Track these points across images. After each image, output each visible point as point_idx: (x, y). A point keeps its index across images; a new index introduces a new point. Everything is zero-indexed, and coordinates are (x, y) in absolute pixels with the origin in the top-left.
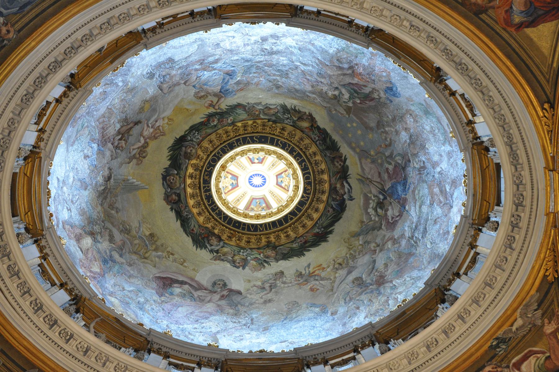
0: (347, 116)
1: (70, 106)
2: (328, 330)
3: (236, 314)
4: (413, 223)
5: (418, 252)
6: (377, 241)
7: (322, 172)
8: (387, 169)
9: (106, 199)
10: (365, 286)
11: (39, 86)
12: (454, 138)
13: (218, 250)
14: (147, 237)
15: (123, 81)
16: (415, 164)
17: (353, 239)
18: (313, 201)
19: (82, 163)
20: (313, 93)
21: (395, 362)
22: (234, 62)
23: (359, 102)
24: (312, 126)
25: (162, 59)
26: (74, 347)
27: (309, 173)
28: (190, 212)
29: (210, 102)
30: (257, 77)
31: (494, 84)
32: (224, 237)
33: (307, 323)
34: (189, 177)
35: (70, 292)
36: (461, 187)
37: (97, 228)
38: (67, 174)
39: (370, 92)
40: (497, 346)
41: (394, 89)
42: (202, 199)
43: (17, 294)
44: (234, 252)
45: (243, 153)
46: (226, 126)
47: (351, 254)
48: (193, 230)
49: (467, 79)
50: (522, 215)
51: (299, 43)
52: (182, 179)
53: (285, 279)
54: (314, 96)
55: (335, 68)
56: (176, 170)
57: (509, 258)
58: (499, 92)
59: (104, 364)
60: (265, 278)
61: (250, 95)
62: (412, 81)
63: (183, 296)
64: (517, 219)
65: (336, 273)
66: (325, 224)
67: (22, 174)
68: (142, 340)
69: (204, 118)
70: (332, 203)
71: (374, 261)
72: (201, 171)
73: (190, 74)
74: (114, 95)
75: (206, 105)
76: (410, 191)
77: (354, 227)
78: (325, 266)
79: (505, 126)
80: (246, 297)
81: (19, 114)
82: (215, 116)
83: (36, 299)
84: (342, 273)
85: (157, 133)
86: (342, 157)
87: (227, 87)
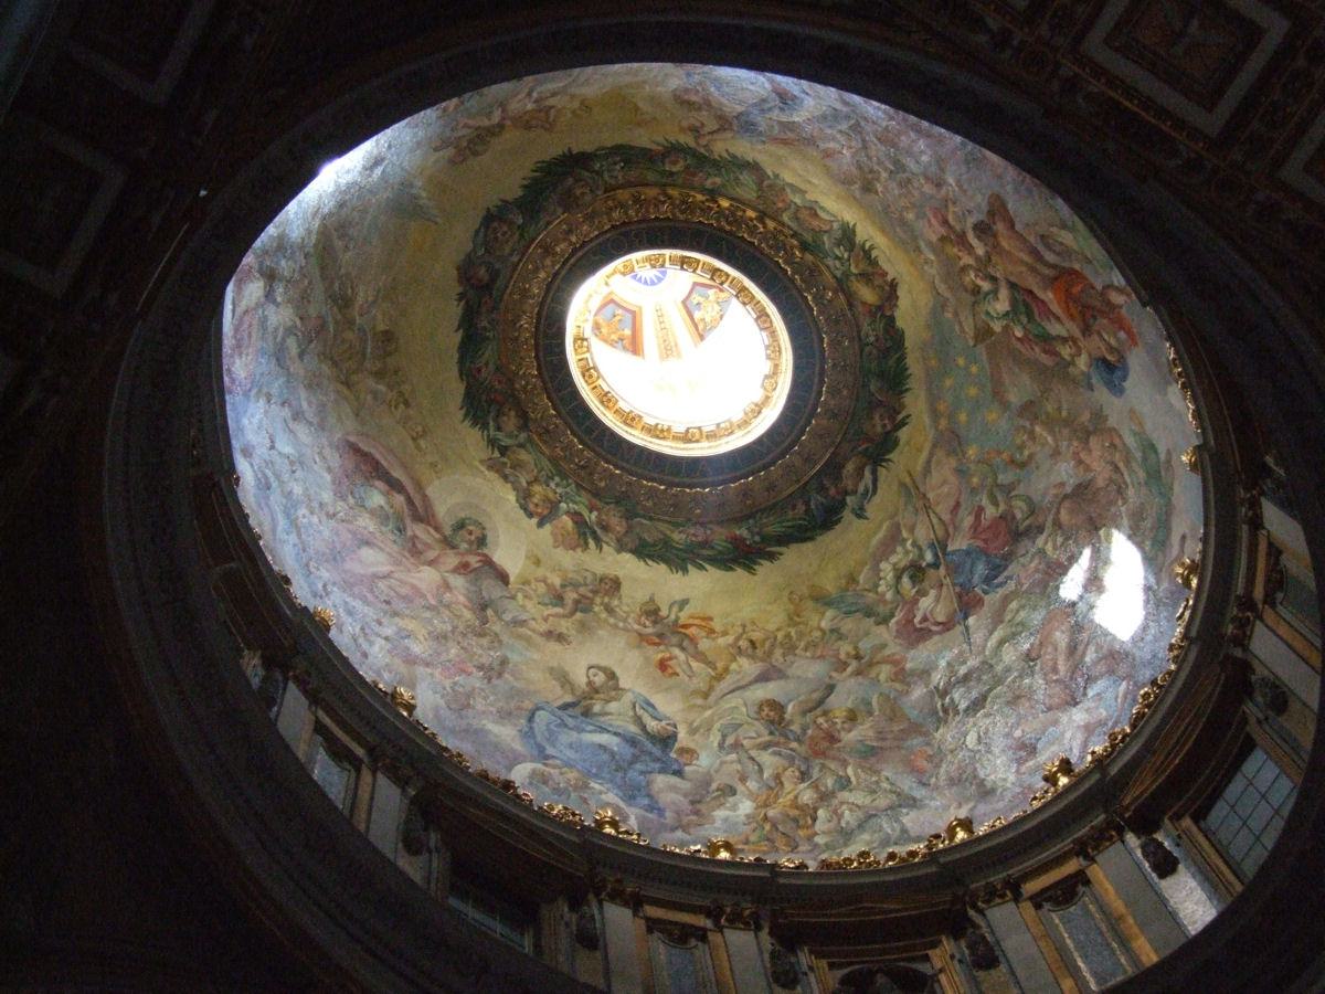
0: (971, 343)
5: (937, 735)
6: (860, 645)
8: (981, 509)
17: (810, 604)
23: (1019, 334)
29: (698, 124)
30: (839, 142)
44: (539, 472)
46: (693, 189)
48: (479, 371)
52: (523, 243)
53: (616, 602)
54: (933, 258)
56: (523, 218)
61: (796, 163)
69: (658, 144)
71: (831, 688)
75: (685, 124)
76: (1001, 592)
77: (830, 583)
78: (717, 625)
80: (513, 598)
84: (747, 667)
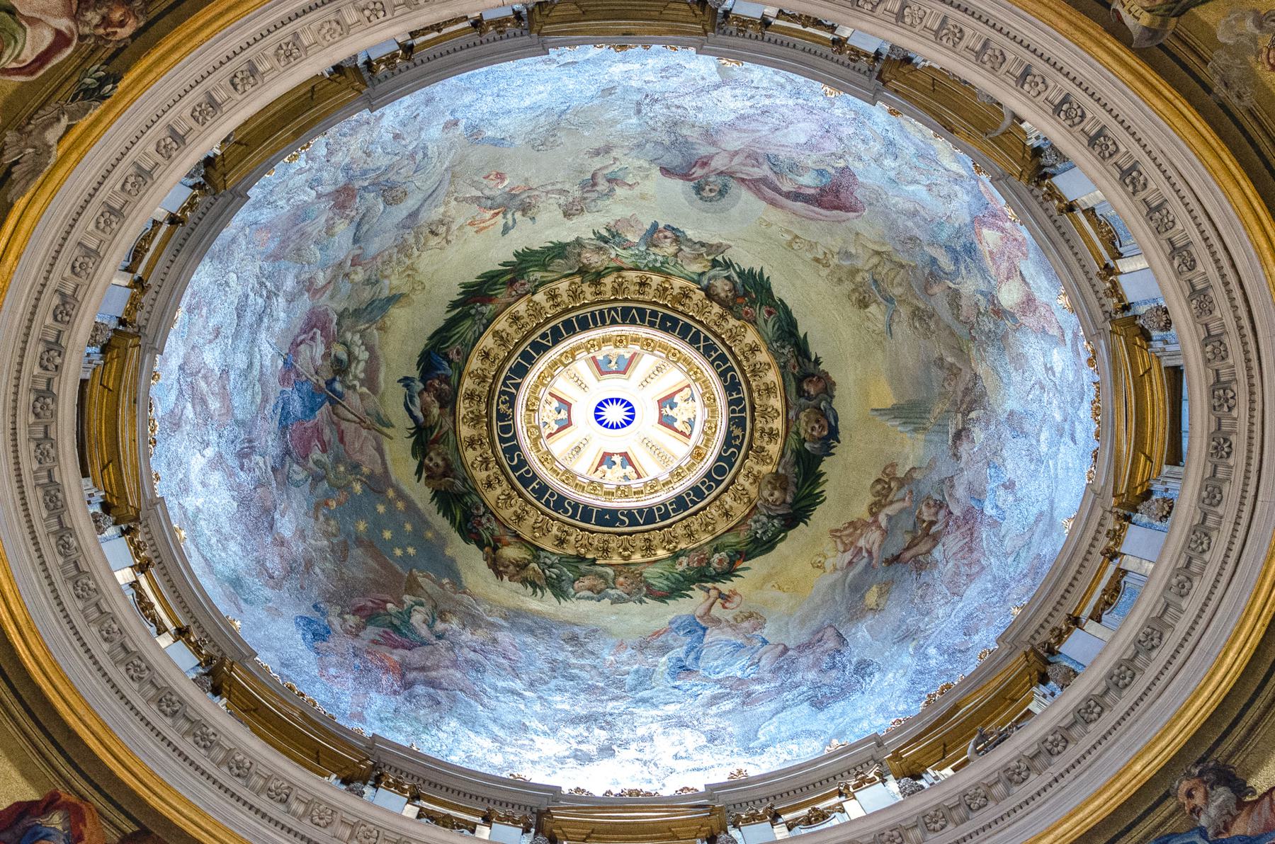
1: (1048, 608)
2: (467, 89)
3: (675, 124)
4: (268, 328)
5: (258, 263)
7: (472, 443)
8: (324, 451)
9: (967, 389)
10: (379, 184)
11: (1123, 668)
12: (176, 526)
13: (714, 267)
14: (875, 301)
15: (927, 657)
16: (261, 464)
17: (405, 290)
18: (494, 376)
19: (1019, 472)
20: (493, 625)
21: (328, 37)
22: (674, 699)
23: (389, 606)
24: (495, 549)
25: (838, 707)
26: (1051, 83)
27: (502, 440)
28: (775, 354)
29: (727, 605)
31: (100, 669)
32: (699, 295)
33: (513, 103)
34: (777, 434)
35: (1053, 194)
36: (160, 414)
37: (988, 324)
38: (1054, 449)
39: (364, 628)
40: (102, 82)
41: (309, 636)
42: (748, 382)
43: (1176, 207)
44: (677, 262)
45: (653, 486)
46: (693, 550)
47: (409, 256)
48: (770, 313)
49: (160, 680)
50: (37, 370)
51: (527, 742)
52: (794, 429)
54: (489, 619)
55: (445, 685)
57: (68, 272)
58: (88, 651)
59: (985, 45)
60: (608, 202)
61: (637, 621)
62: (270, 655)
63: (794, 167)
64: (48, 360)
65: (444, 214)
66: (468, 323)
67: (1156, 460)
68: (894, 84)
70: (450, 372)
71: (356, 240)
72: (750, 447)
73: (775, 671)
74: (947, 626)
75: (737, 599)
76: (272, 402)
77: (399, 316)
78: (470, 231)
79: (75, 573)
81: (1168, 605)
82: (718, 574)
83: (1134, 194)
85: (850, 535)
86: (428, 477)
87: (689, 640)
